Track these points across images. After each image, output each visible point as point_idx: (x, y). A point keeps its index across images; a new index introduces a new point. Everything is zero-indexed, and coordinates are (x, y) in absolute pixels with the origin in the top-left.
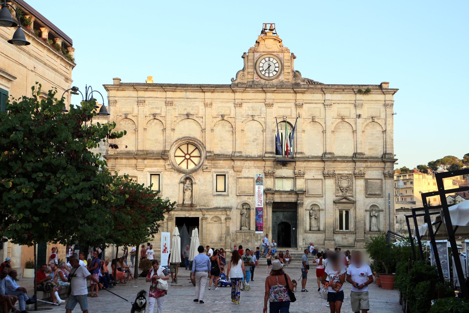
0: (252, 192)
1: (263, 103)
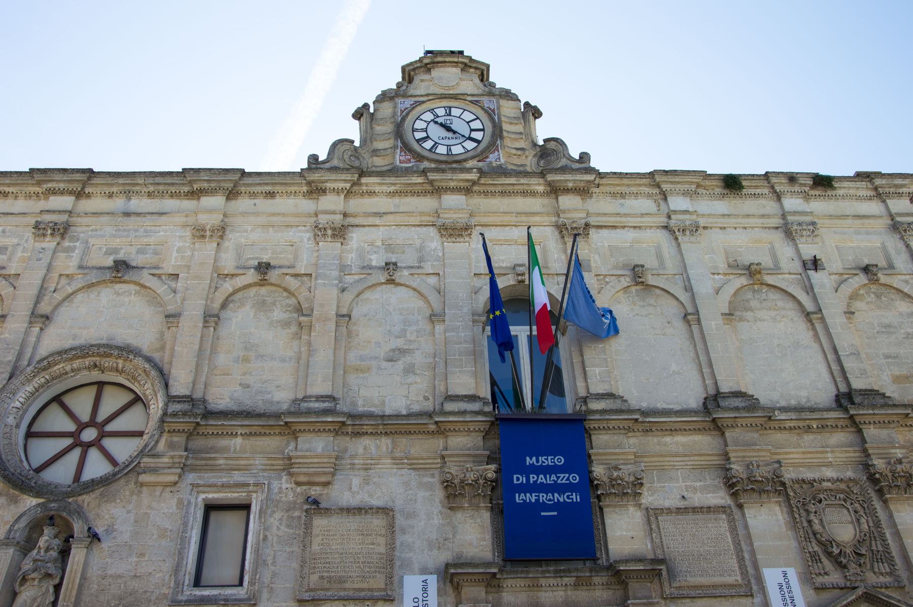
1: (432, 228)
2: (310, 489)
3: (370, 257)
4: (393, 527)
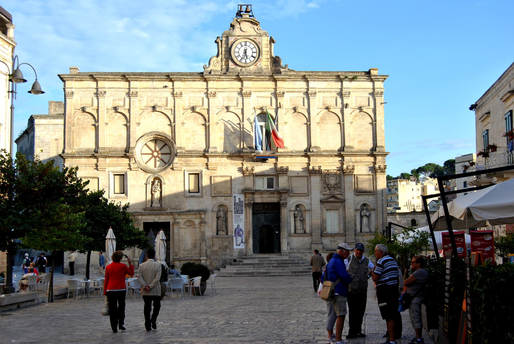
0: (229, 192)
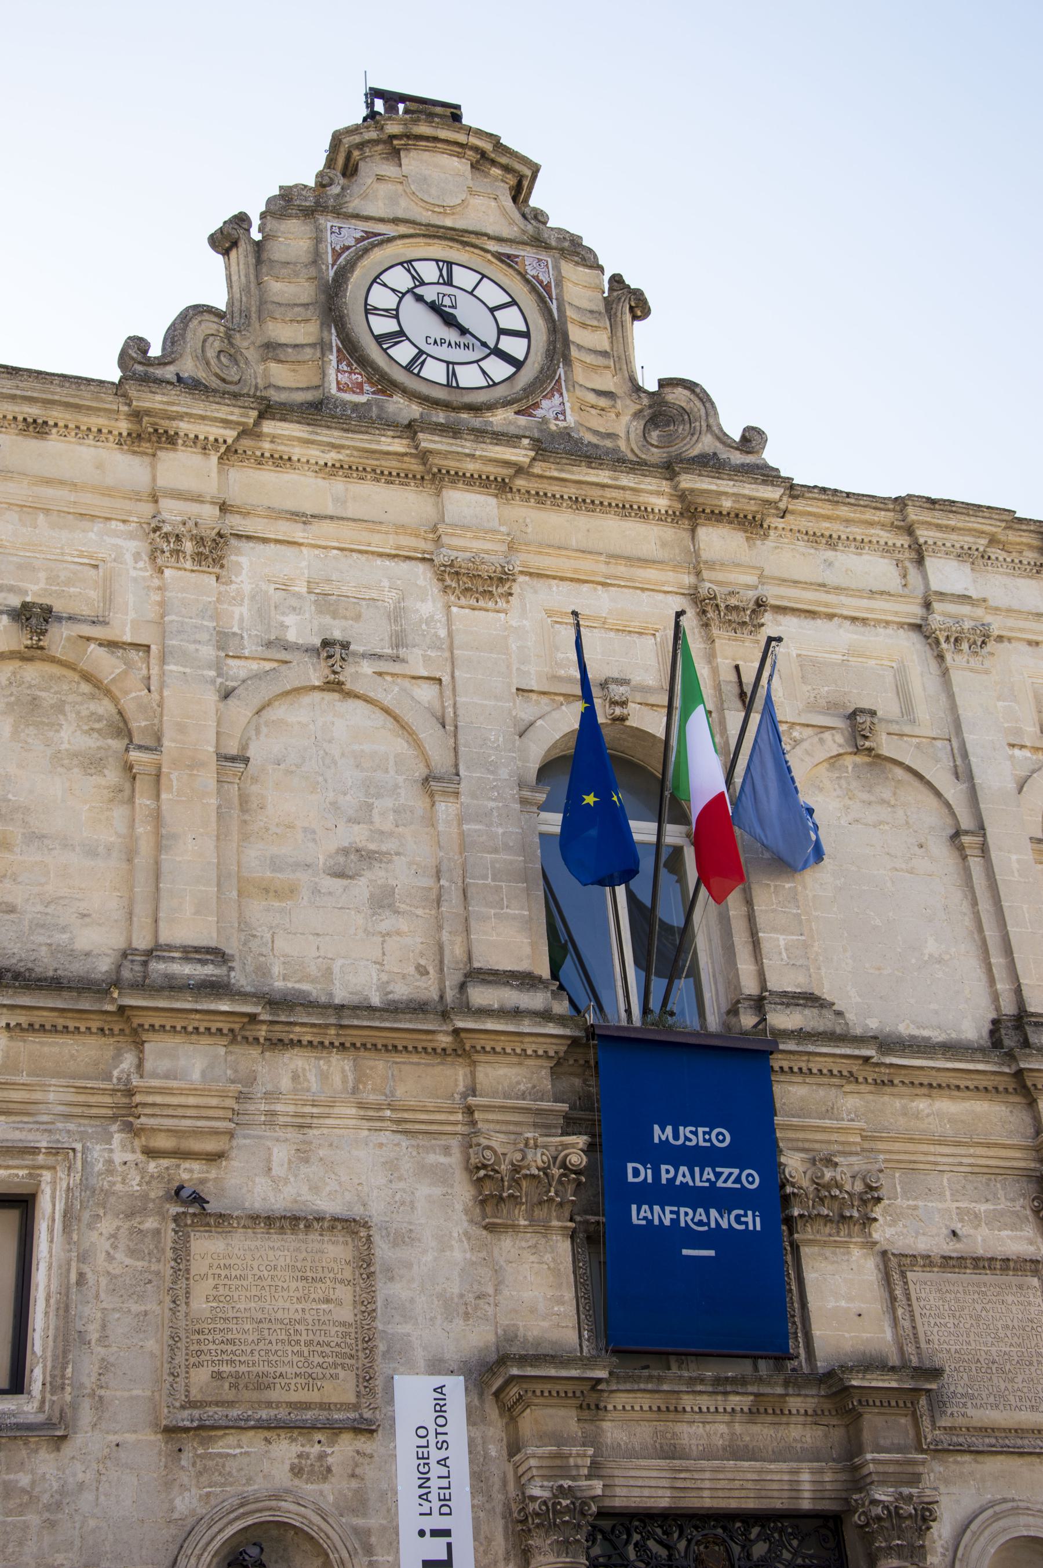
1: (421, 568)
2: (178, 1166)
3: (282, 618)
4: (369, 1265)
